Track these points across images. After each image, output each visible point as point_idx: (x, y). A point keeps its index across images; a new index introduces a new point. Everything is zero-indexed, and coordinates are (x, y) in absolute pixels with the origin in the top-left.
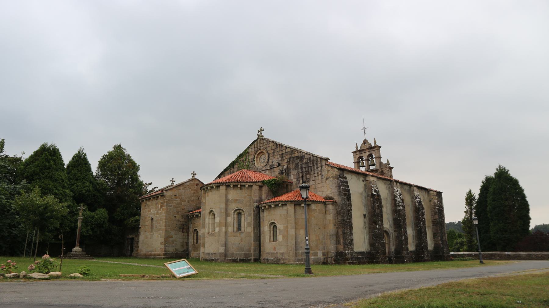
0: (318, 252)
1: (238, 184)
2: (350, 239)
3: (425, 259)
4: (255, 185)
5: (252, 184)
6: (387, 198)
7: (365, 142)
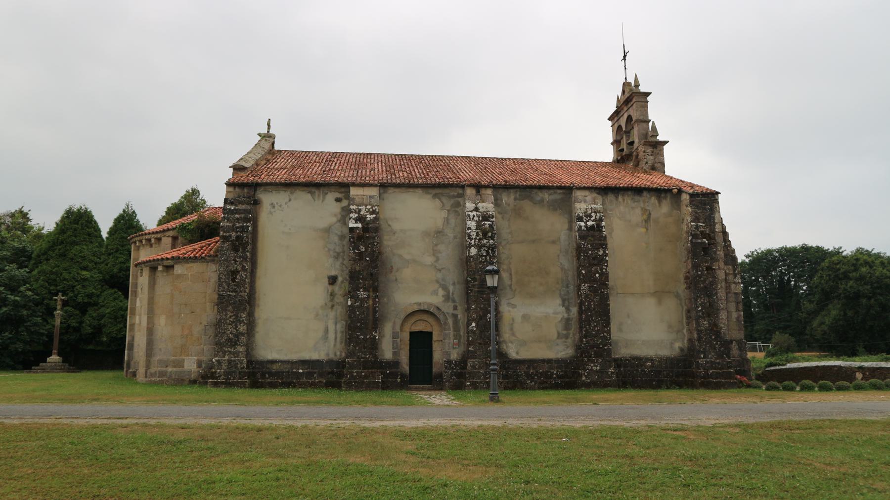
0: (184, 360)
1: (141, 239)
2: (231, 333)
3: (584, 381)
4: (164, 236)
5: (159, 236)
6: (439, 233)
7: (626, 84)
